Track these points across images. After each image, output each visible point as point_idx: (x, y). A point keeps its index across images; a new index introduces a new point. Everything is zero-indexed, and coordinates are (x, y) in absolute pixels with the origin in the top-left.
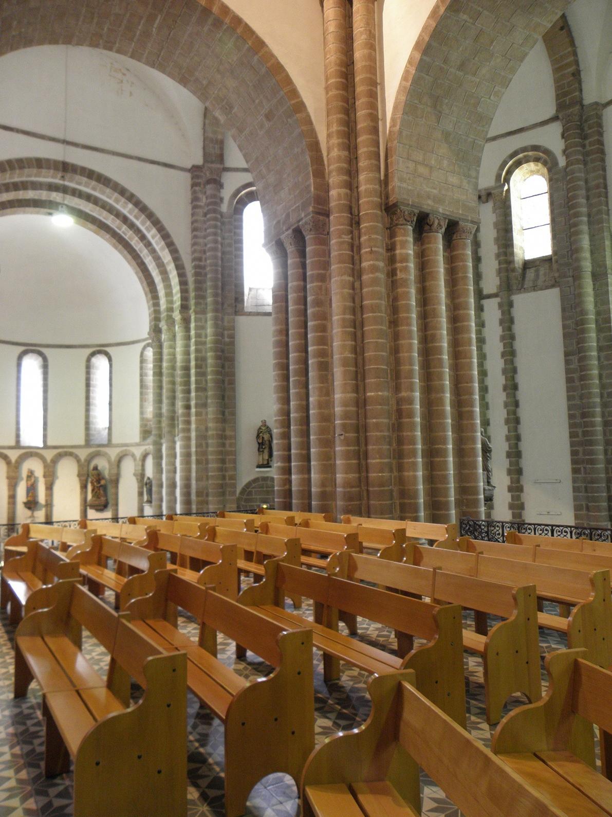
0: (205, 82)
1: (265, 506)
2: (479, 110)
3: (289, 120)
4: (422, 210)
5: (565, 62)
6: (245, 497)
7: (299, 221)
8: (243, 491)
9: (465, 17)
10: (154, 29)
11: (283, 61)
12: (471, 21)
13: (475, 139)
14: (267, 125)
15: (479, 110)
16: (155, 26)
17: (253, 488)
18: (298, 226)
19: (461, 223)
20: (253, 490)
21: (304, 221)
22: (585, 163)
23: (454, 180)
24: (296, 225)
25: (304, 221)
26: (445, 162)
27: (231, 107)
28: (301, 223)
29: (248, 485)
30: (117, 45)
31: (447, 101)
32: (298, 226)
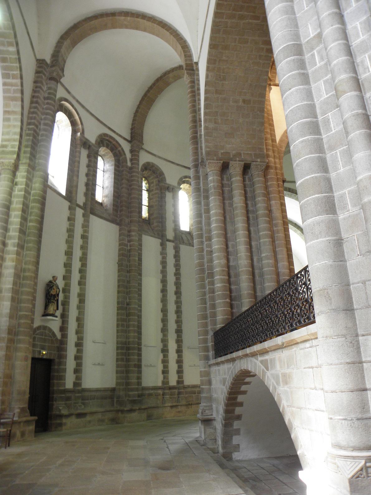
0: (224, 58)
1: (44, 353)
3: (258, 112)
7: (253, 162)
10: (247, 21)
14: (241, 103)
16: (250, 21)
17: (36, 335)
18: (251, 163)
20: (37, 336)
21: (258, 163)
24: (249, 162)
25: (258, 163)
27: (224, 79)
28: (254, 163)
30: (225, 3)
32: (251, 163)
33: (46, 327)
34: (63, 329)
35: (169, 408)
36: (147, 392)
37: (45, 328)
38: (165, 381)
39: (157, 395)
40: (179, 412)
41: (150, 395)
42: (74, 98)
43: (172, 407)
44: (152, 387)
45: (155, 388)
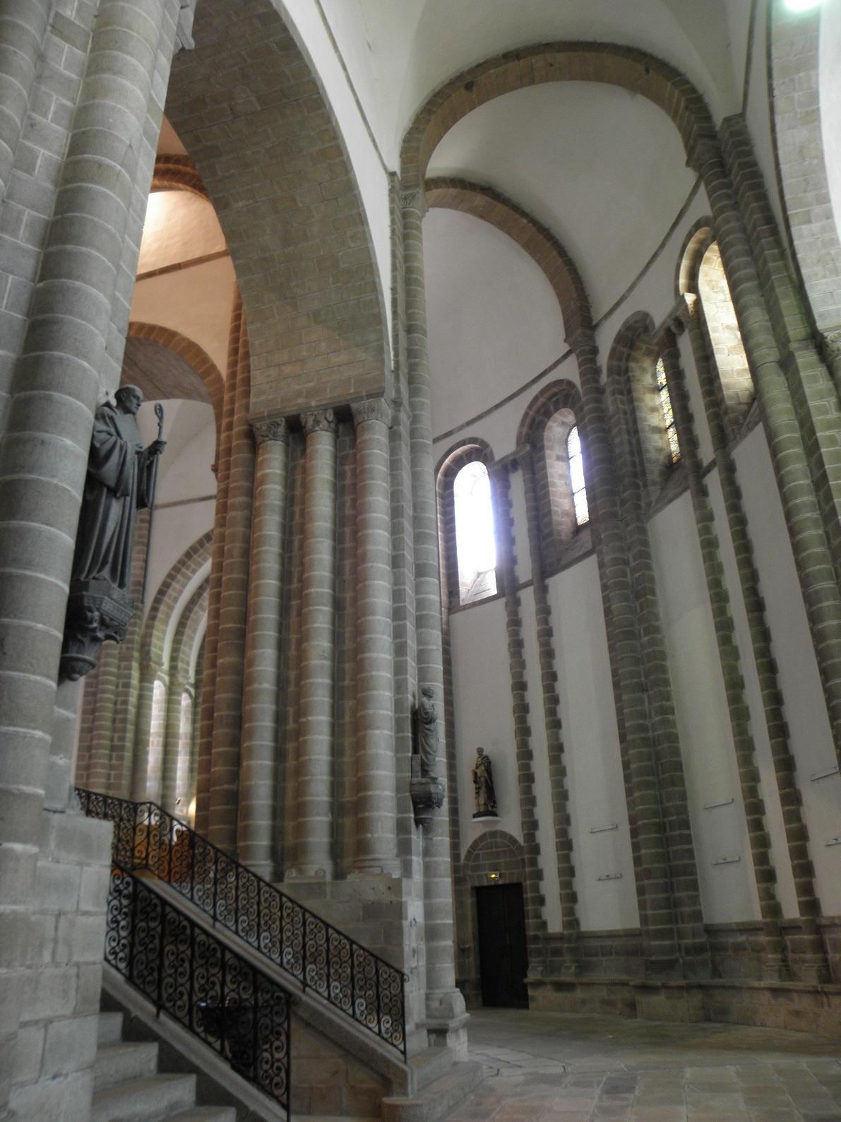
1: (493, 876)
2: (343, 266)
4: (286, 415)
5: (675, 100)
6: (471, 863)
8: (469, 853)
9: (241, 204)
11: (194, 338)
12: (251, 202)
13: (358, 299)
15: (343, 266)
17: (480, 849)
19: (354, 406)
20: (481, 852)
22: (735, 206)
23: (342, 358)
26: (323, 345)
29: (475, 845)
31: (294, 283)
33: (496, 832)
34: (531, 826)
35: (767, 995)
36: (731, 940)
37: (494, 834)
38: (772, 907)
39: (758, 949)
40: (797, 1013)
41: (739, 948)
42: (461, 428)
43: (775, 991)
44: (737, 924)
45: (749, 929)
